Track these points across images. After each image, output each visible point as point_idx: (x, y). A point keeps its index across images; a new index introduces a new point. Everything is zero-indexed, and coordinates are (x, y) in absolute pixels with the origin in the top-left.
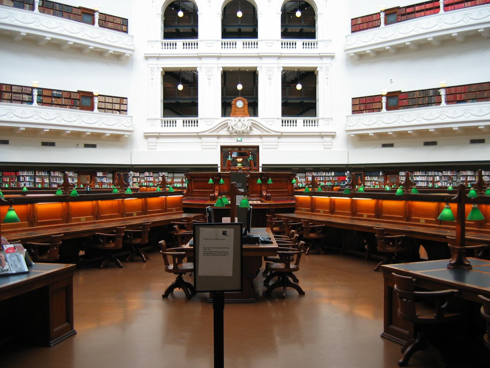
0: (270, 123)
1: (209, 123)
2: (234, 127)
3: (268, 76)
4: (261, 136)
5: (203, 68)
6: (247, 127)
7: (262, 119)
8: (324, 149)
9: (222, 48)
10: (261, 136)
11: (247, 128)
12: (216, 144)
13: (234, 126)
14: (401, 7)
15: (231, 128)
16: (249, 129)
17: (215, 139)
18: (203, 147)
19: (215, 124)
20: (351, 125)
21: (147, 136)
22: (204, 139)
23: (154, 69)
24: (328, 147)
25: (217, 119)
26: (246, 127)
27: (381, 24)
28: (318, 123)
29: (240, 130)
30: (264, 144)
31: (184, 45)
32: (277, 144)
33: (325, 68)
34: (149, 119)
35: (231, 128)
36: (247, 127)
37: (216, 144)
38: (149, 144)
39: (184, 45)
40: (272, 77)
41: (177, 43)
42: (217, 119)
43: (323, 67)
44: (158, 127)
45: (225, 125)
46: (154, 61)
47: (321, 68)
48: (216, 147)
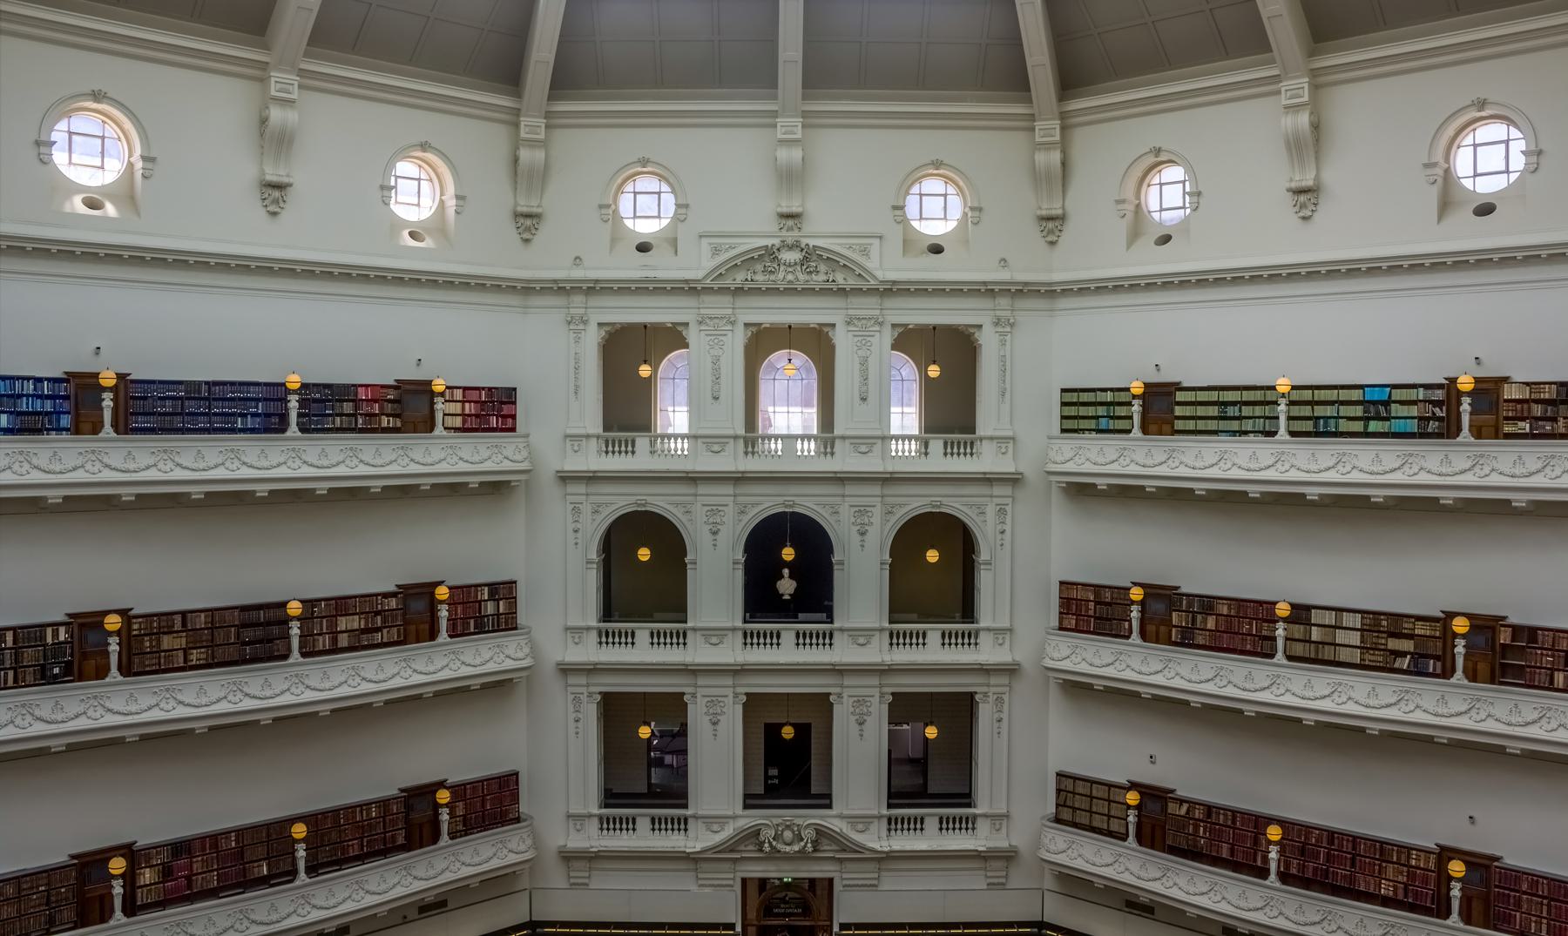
0: (860, 827)
1: (715, 827)
2: (774, 843)
3: (858, 717)
4: (840, 860)
5: (699, 695)
6: (807, 842)
7: (841, 817)
8: (988, 885)
9: (745, 644)
10: (840, 860)
11: (805, 846)
12: (731, 876)
13: (774, 839)
14: (1185, 384)
15: (766, 845)
16: (809, 847)
17: (727, 866)
18: (700, 882)
19: (728, 831)
20: (1052, 847)
21: (569, 857)
22: (705, 866)
23: (581, 696)
24: (996, 881)
25: (734, 817)
26: (802, 844)
27: (1132, 633)
28: (973, 824)
29: (788, 849)
30: (845, 876)
31: (652, 638)
32: (876, 875)
33: (995, 697)
34: (572, 816)
35: (766, 845)
36: (807, 842)
37: (731, 876)
38: (572, 874)
39: (652, 638)
40: (865, 717)
41: (638, 633)
42: (734, 817)
43: (990, 694)
44: (592, 839)
45: (754, 834)
46: (583, 680)
47: (985, 694)
48: (731, 882)
